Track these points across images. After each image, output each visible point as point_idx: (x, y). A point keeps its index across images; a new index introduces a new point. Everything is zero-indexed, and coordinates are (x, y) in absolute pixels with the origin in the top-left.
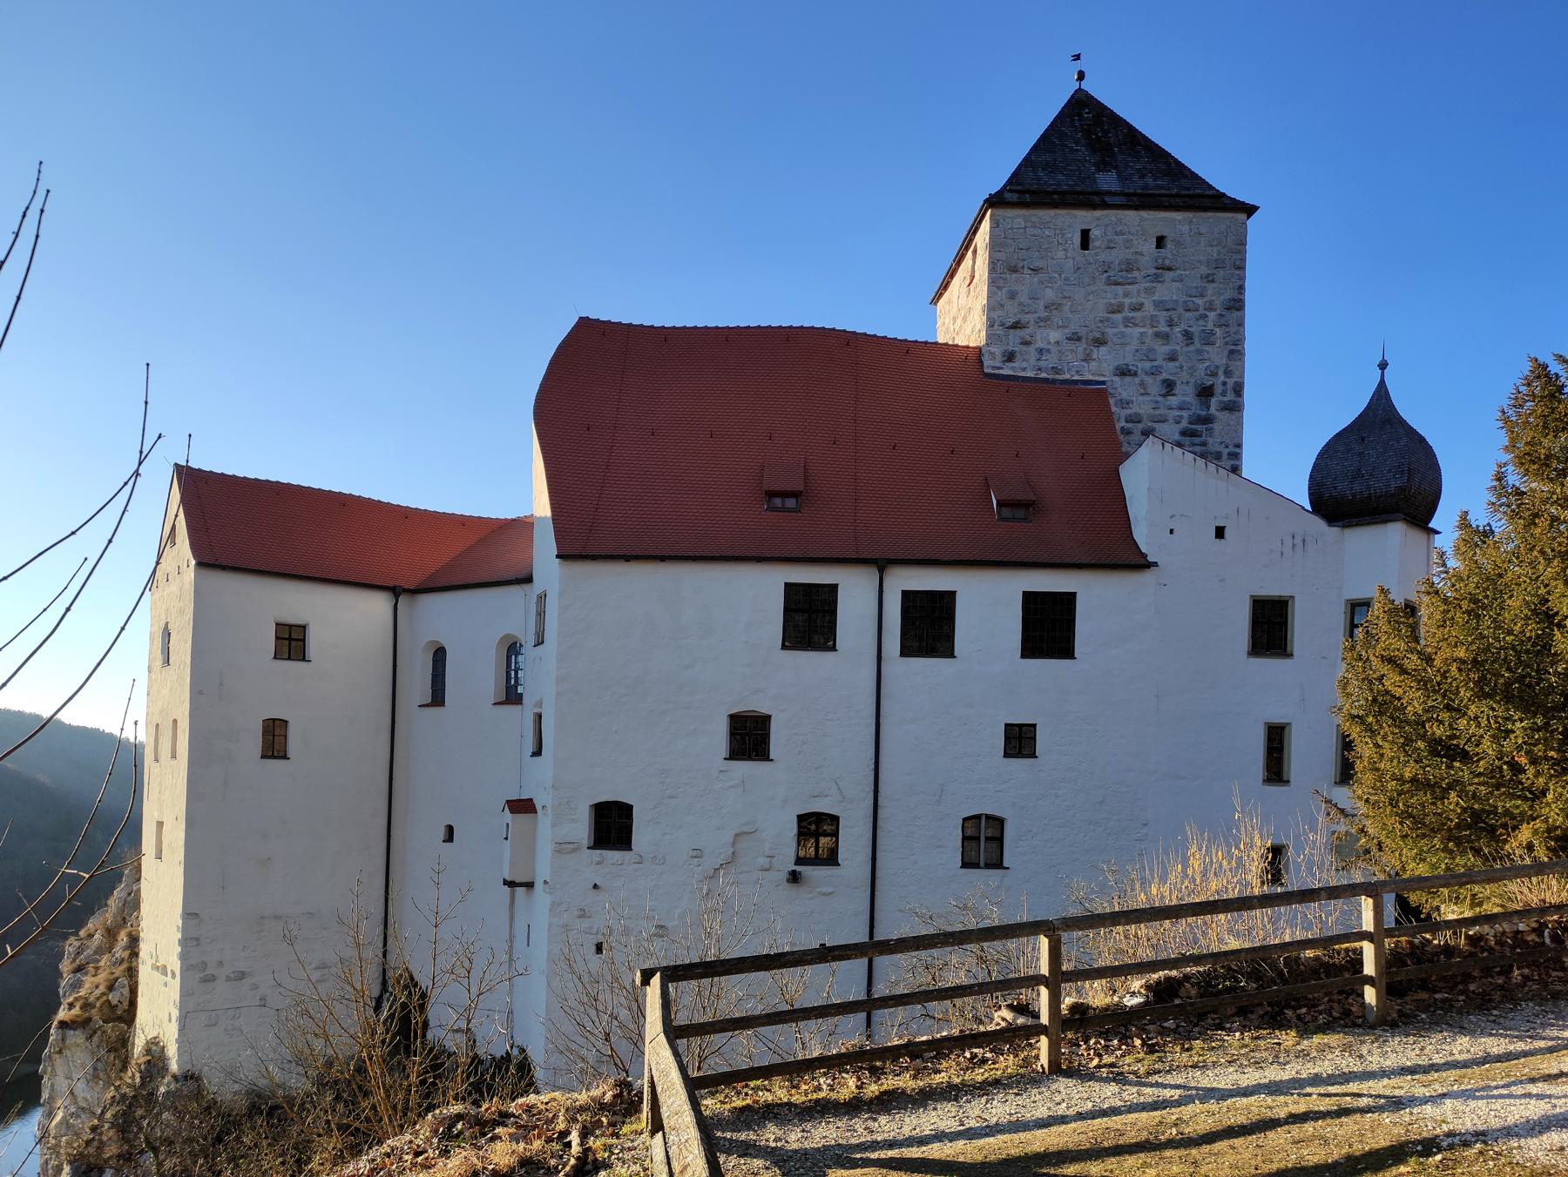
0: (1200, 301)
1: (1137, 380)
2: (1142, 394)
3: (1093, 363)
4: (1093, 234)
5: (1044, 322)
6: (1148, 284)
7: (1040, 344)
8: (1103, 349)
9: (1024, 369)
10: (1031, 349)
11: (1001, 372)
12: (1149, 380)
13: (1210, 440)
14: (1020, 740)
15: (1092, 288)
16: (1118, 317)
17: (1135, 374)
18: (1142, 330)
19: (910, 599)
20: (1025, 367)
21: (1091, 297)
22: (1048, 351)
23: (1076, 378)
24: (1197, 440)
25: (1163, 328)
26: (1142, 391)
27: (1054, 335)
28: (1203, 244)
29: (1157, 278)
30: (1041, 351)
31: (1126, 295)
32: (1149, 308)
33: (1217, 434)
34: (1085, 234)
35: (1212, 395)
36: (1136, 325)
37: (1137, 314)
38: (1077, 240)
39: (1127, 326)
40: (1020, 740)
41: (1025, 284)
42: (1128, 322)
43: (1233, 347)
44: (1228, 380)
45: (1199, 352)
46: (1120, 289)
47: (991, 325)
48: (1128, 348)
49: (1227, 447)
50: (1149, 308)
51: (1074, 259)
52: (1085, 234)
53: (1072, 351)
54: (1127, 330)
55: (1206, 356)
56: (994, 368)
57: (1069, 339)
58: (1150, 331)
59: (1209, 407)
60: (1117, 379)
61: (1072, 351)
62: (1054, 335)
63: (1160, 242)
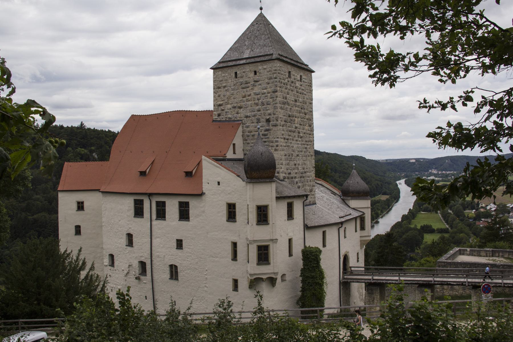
0: (265, 91)
1: (250, 118)
2: (252, 123)
3: (239, 114)
4: (238, 73)
5: (227, 103)
6: (252, 87)
7: (226, 110)
8: (242, 109)
9: (223, 118)
10: (224, 112)
11: (217, 119)
12: (253, 118)
13: (270, 136)
14: (179, 244)
15: (238, 91)
16: (245, 99)
17: (250, 117)
18: (251, 102)
19: (158, 203)
20: (223, 118)
21: (238, 93)
22: (228, 112)
23: (235, 119)
24: (266, 137)
25: (257, 101)
26: (252, 122)
27: (229, 106)
28: (266, 72)
29: (254, 85)
30: (226, 112)
31: (247, 91)
32: (252, 94)
33: (272, 134)
34: (236, 73)
35: (270, 121)
36: (249, 101)
37: (250, 97)
38: (234, 76)
39: (247, 101)
40: (179, 244)
41: (222, 92)
42: (248, 100)
43: (275, 105)
44: (274, 116)
45: (266, 108)
46: (245, 90)
47: (214, 106)
48: (248, 108)
49: (275, 138)
50: (252, 94)
51: (233, 82)
52: (236, 73)
53: (234, 111)
54: (248, 103)
55: (268, 108)
56: (216, 119)
57: (233, 107)
58: (253, 102)
59: (269, 125)
60: (245, 119)
61: (234, 111)
62: (229, 106)
63: (255, 73)
